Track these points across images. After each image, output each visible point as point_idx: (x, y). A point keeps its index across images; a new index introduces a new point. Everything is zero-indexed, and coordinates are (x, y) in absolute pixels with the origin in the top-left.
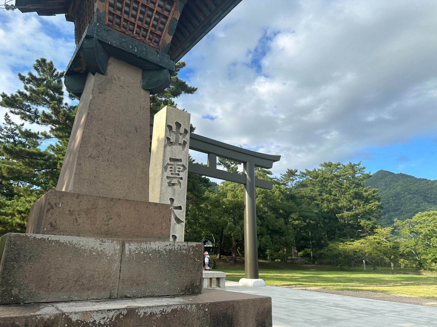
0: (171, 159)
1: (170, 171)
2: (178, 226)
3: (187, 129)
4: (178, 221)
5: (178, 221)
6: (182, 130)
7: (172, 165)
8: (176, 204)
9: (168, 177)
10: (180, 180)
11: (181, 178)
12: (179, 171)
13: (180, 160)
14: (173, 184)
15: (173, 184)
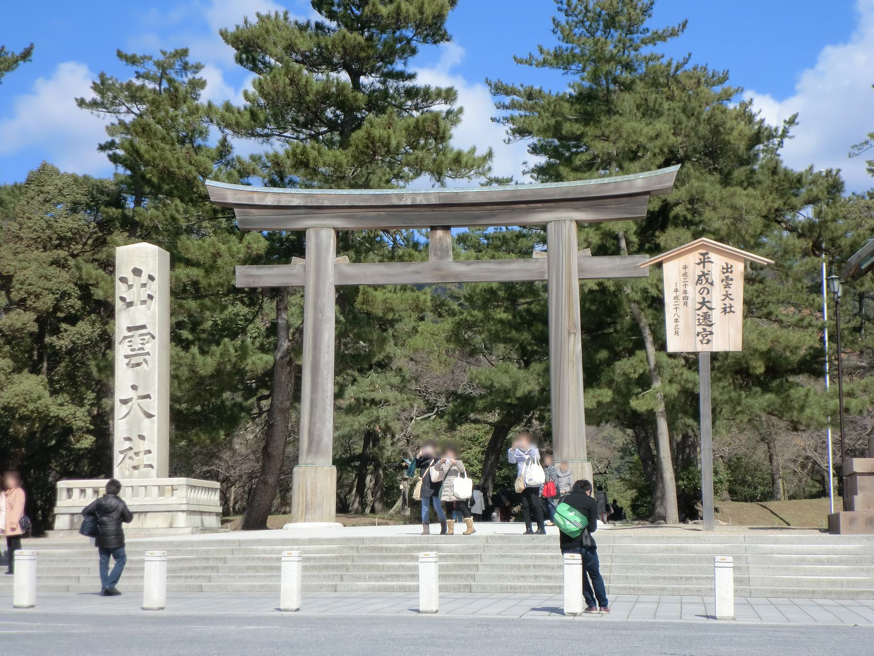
0: (129, 329)
1: (130, 346)
2: (147, 421)
3: (152, 274)
4: (150, 416)
5: (150, 416)
6: (144, 278)
7: (132, 336)
8: (141, 392)
9: (126, 357)
10: (147, 357)
11: (148, 354)
12: (143, 344)
13: (144, 327)
14: (138, 365)
15: (138, 365)
